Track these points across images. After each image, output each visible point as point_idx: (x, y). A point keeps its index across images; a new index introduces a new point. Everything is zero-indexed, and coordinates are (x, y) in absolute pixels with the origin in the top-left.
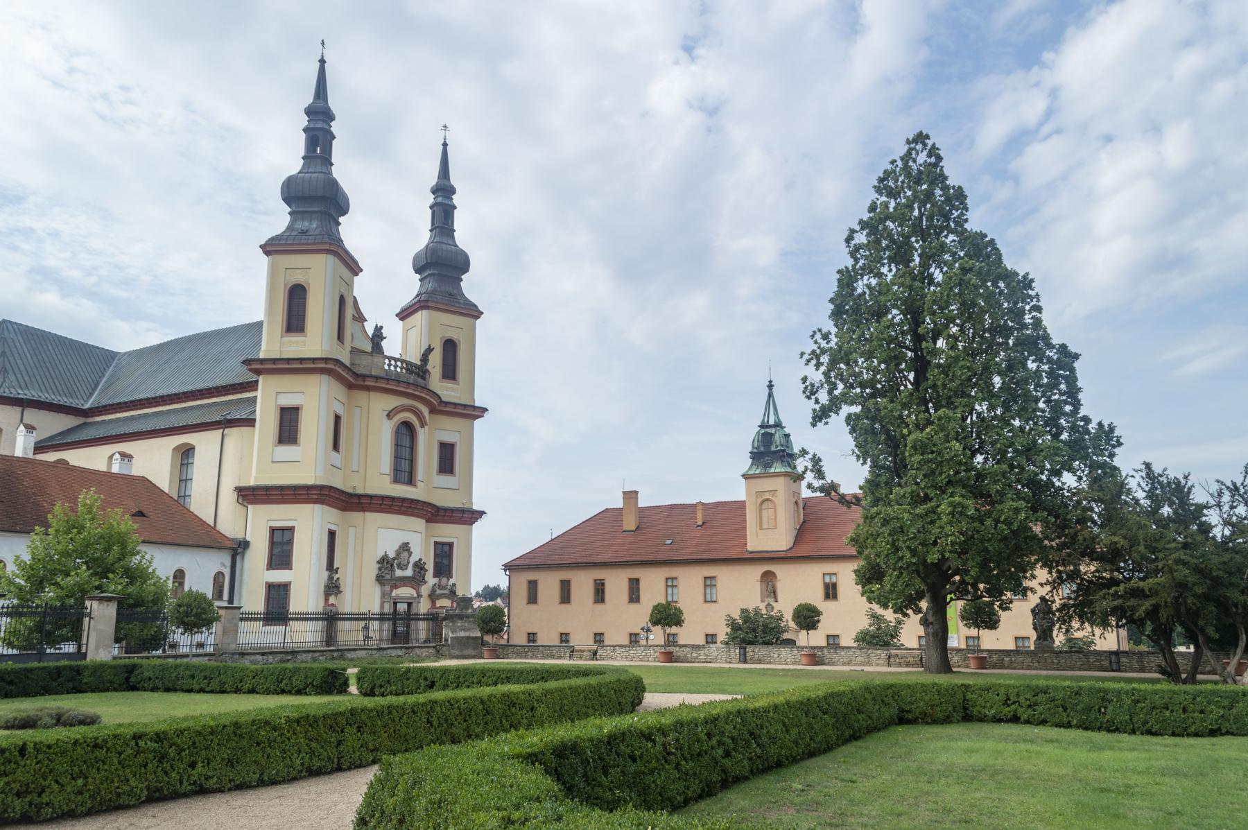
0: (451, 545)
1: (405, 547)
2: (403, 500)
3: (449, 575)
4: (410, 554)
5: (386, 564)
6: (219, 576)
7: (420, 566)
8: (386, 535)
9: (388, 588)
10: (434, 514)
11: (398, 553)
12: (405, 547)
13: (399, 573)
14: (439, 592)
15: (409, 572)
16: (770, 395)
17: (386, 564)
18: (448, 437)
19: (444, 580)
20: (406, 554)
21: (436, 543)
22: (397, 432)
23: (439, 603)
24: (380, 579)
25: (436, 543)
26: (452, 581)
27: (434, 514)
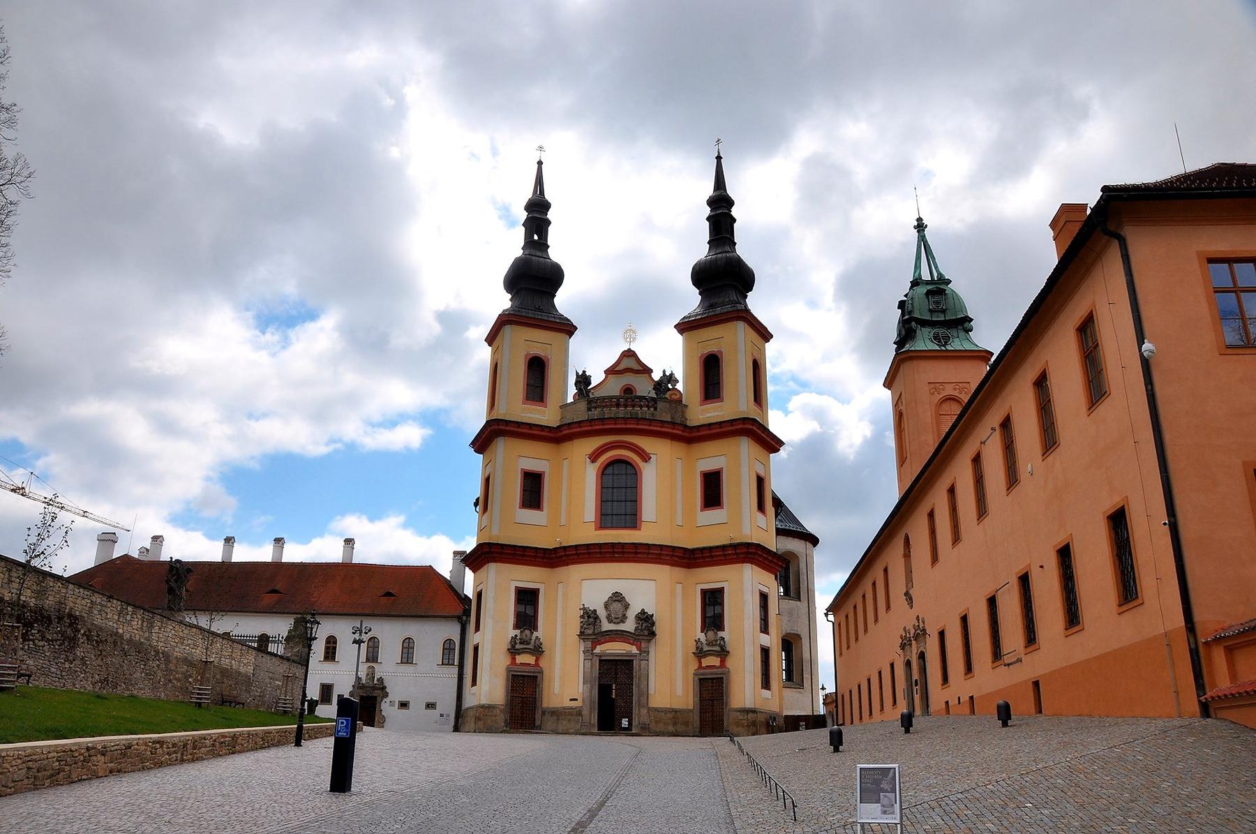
0: (720, 591)
1: (617, 598)
2: (613, 545)
3: (721, 628)
4: (627, 606)
5: (590, 617)
6: (448, 647)
7: (645, 620)
8: (592, 587)
9: (589, 644)
10: (689, 558)
11: (606, 606)
12: (617, 598)
13: (606, 626)
14: (706, 648)
15: (630, 626)
16: (922, 239)
17: (590, 617)
18: (709, 465)
19: (710, 634)
20: (616, 606)
21: (704, 592)
22: (603, 472)
23: (707, 661)
24: (582, 634)
25: (704, 592)
26: (721, 634)
27: (689, 558)
